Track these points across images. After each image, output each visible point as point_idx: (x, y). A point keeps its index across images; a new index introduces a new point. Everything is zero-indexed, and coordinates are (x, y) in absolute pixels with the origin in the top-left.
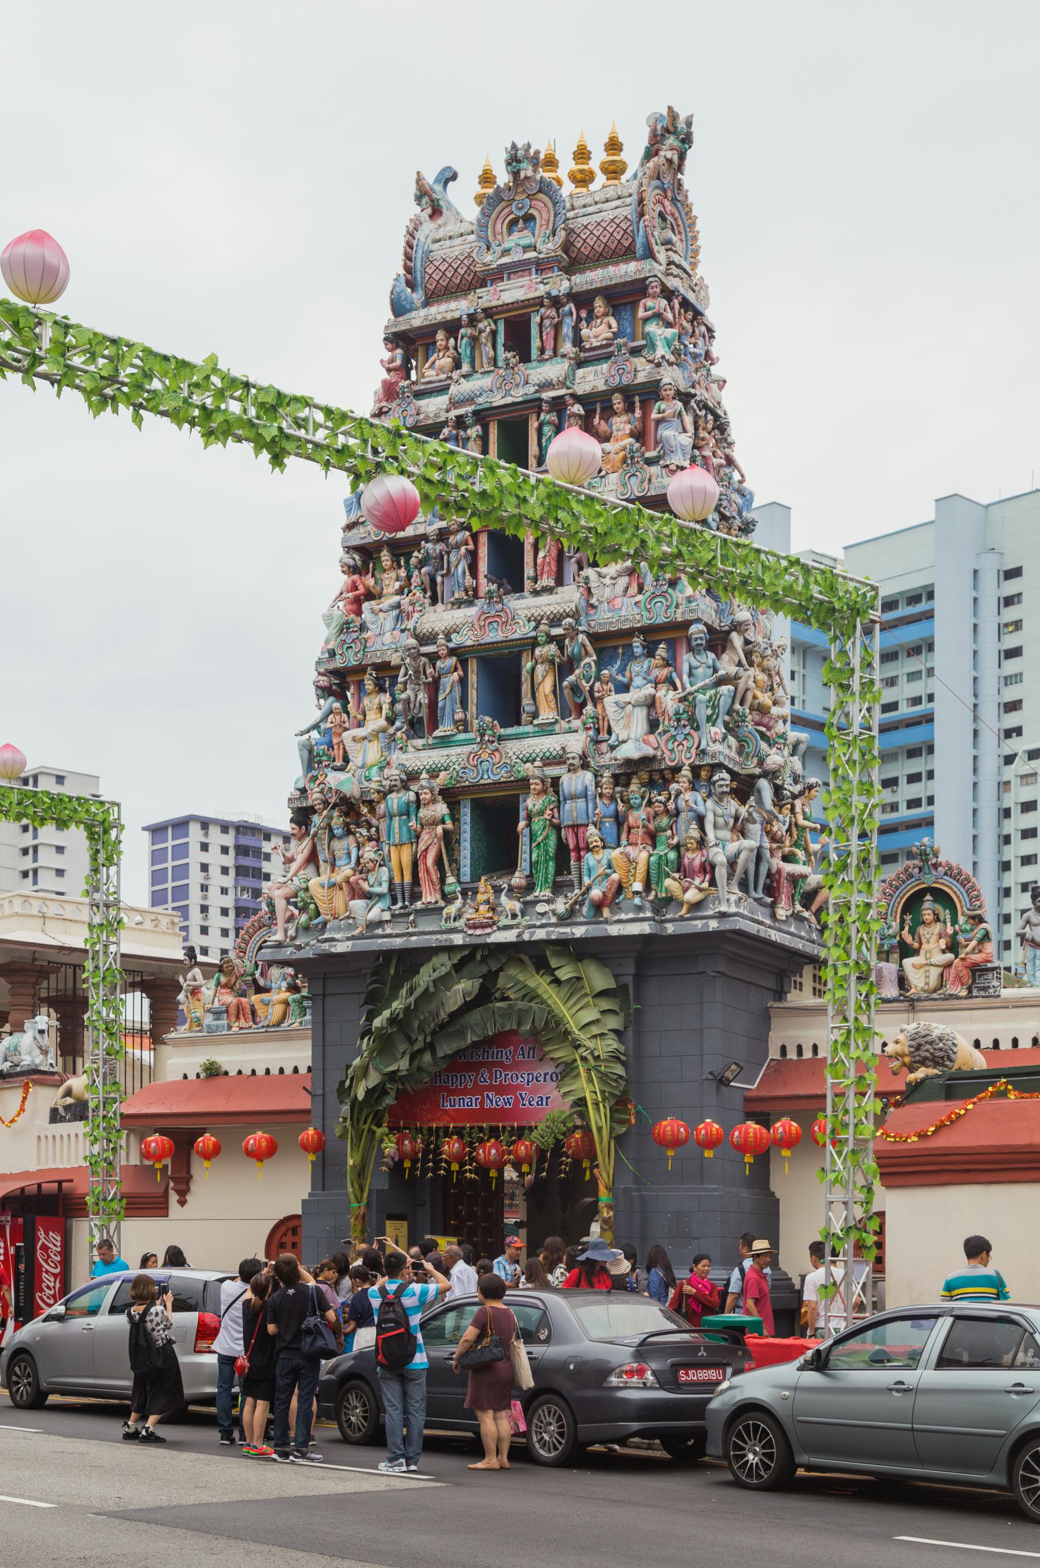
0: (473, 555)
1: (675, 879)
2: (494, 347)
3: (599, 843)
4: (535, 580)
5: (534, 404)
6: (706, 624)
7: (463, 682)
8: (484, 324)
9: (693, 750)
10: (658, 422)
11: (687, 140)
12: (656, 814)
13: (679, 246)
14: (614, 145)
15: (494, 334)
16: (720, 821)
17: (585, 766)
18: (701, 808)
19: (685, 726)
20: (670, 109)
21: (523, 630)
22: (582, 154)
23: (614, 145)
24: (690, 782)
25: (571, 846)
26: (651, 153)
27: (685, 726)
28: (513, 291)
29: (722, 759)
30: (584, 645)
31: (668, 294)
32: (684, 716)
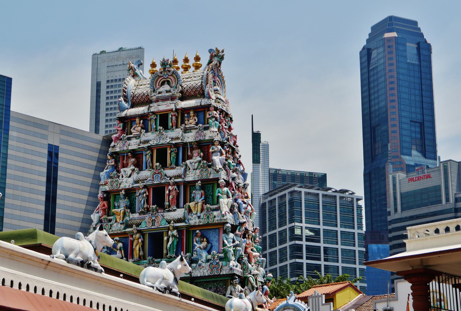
0: (148, 196)
2: (156, 124)
5: (170, 145)
7: (143, 242)
8: (153, 117)
10: (213, 153)
11: (222, 58)
13: (220, 92)
14: (197, 58)
15: (156, 120)
20: (216, 48)
21: (164, 224)
22: (186, 60)
23: (197, 58)
26: (210, 62)
28: (163, 107)
31: (216, 109)
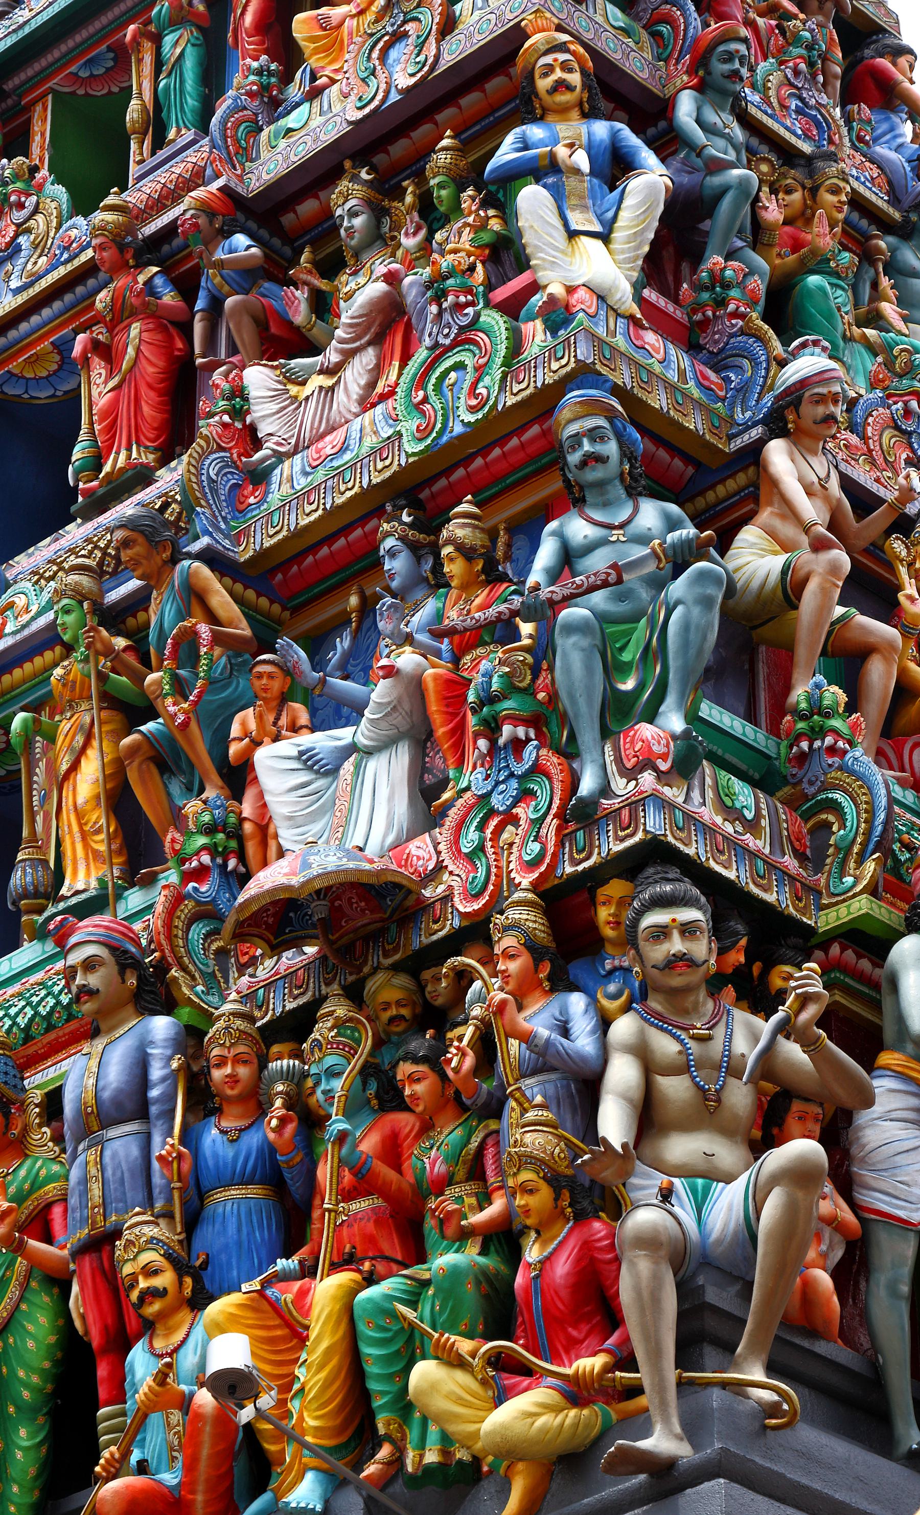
1: (457, 1362)
3: (166, 1279)
4: (96, 462)
6: (618, 391)
9: (550, 826)
12: (427, 1127)
16: (675, 1088)
17: (154, 995)
18: (583, 1041)
19: (518, 745)
24: (532, 947)
25: (95, 1341)
27: (518, 745)
29: (653, 822)
30: (194, 597)
32: (508, 705)
